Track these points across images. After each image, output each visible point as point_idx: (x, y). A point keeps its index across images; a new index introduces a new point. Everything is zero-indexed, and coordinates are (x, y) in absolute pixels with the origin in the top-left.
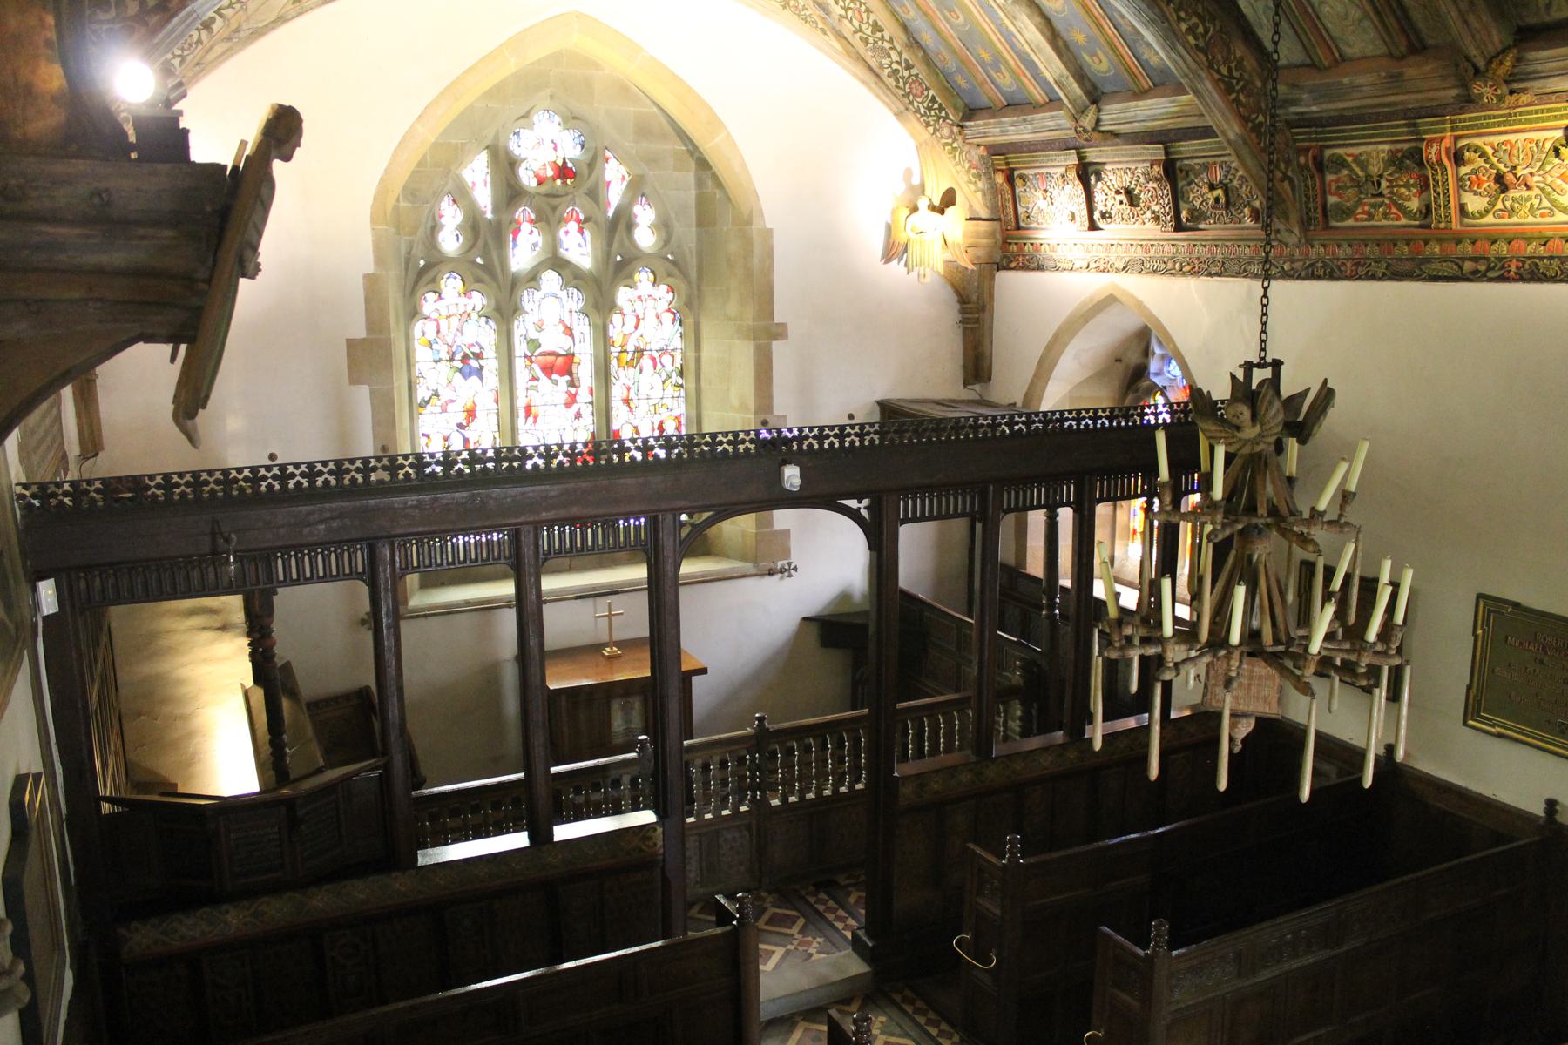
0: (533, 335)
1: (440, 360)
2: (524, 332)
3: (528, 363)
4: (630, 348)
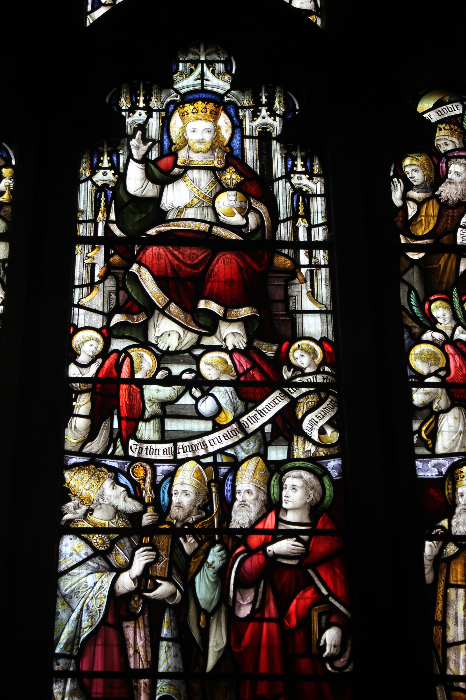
3: (116, 259)
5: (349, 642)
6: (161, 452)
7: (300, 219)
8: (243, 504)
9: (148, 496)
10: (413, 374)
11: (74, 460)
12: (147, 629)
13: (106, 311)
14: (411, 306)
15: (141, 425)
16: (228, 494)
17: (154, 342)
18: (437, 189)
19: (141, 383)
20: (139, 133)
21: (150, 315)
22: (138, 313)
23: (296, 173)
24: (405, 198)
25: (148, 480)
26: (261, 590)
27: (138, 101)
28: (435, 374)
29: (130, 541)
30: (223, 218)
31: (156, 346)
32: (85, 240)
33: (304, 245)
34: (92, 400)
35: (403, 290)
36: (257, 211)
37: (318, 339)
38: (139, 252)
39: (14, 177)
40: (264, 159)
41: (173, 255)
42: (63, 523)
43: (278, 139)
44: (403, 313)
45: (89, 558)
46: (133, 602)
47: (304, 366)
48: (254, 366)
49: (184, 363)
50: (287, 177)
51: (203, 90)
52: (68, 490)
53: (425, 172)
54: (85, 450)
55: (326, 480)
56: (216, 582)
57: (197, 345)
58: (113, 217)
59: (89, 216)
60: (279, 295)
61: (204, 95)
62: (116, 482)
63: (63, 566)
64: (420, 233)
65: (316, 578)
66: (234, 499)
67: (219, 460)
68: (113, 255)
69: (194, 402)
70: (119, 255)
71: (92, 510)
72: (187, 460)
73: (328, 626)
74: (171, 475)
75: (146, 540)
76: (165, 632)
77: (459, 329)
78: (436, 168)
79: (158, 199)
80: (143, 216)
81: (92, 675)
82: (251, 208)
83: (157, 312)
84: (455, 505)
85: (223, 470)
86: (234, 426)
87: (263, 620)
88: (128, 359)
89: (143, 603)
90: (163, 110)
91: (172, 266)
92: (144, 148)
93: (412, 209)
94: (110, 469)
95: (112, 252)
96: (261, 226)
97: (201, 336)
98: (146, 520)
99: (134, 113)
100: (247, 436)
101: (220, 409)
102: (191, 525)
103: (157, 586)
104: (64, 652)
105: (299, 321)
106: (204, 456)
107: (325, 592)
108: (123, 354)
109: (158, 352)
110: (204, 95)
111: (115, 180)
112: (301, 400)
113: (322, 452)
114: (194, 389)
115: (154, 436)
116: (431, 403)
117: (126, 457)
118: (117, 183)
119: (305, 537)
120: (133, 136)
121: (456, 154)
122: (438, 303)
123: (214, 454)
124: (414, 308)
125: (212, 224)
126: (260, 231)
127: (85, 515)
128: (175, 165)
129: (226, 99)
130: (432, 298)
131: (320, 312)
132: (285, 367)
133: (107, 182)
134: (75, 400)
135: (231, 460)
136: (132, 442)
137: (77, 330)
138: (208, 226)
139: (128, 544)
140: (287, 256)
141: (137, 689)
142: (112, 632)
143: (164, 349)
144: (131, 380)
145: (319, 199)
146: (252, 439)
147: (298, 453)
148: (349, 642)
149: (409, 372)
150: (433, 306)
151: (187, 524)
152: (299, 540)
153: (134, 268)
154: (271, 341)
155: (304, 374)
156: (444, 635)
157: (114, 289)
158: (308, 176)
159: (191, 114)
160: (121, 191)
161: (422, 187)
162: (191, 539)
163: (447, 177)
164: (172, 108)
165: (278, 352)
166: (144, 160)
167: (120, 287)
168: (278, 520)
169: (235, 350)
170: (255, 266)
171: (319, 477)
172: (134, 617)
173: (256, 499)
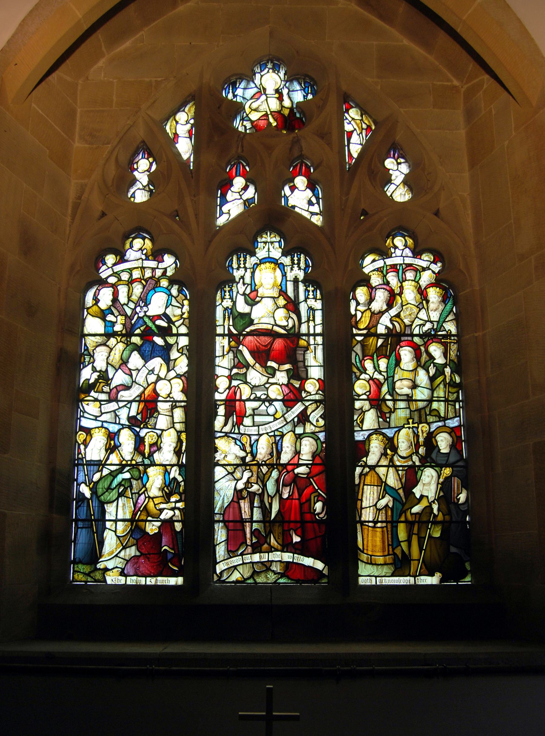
0: (242, 307)
1: (114, 334)
2: (227, 303)
3: (233, 343)
4: (381, 329)
5: (325, 508)
6: (253, 431)
7: (311, 321)
8: (286, 453)
9: (248, 449)
10: (356, 394)
11: (218, 435)
12: (249, 503)
13: (229, 368)
14: (356, 362)
15: (245, 418)
16: (279, 448)
17: (250, 382)
18: (370, 305)
19: (244, 401)
20: (242, 280)
21: (247, 369)
22: (242, 368)
23: (309, 298)
24: (356, 310)
25: (248, 443)
26: (292, 487)
27: (240, 264)
28: (365, 394)
29: (242, 468)
30: (278, 323)
31: (250, 383)
32: (220, 335)
33: (312, 335)
34: (225, 408)
35: (354, 355)
36: (292, 318)
37: (317, 379)
38: (242, 340)
39: (190, 305)
40: (296, 291)
41: (257, 340)
42: (215, 461)
43: (302, 281)
44: (353, 366)
45: (226, 475)
46: (243, 493)
47: (310, 391)
48: (291, 391)
49: (262, 391)
50: (306, 301)
51: (269, 257)
52: (217, 448)
53: (366, 297)
54: (223, 431)
55: (318, 441)
56: (275, 484)
57: (267, 383)
58: (231, 323)
59: (222, 324)
60: (300, 358)
61: (269, 260)
62: (236, 443)
63: (216, 479)
64: (362, 327)
65: (313, 483)
66: (282, 450)
67: (276, 434)
68: (232, 341)
69: (266, 408)
70: (234, 341)
71: (227, 456)
72: (263, 434)
73: (318, 501)
74: (257, 440)
75: (248, 468)
76: (256, 504)
77: (376, 373)
78: (371, 294)
79: (249, 314)
80: (244, 322)
81: (229, 521)
82: (290, 317)
83: (250, 368)
84: (369, 452)
85: (278, 438)
86: (282, 419)
87: (293, 499)
88: (239, 389)
89: (247, 493)
90: (252, 268)
91: (256, 346)
92: (244, 288)
93: (359, 315)
94: (233, 438)
95: (231, 340)
96: (294, 326)
97: (269, 378)
98: (248, 459)
99: (239, 270)
100: (287, 423)
101: (277, 411)
102: (265, 462)
103: (252, 486)
104: (218, 512)
105: (309, 371)
106: (270, 432)
107: (317, 488)
108: (237, 388)
109: (251, 386)
110: (269, 260)
111: (232, 305)
112: (309, 407)
113: (317, 430)
114: (266, 402)
115: (251, 424)
116: (362, 407)
117: (239, 433)
118: (232, 306)
119: (310, 466)
120: (239, 282)
121: (380, 287)
122: (368, 360)
123: (274, 431)
124: (358, 363)
125: (273, 325)
126: (294, 328)
127: (224, 458)
128: (257, 296)
129: (279, 262)
130: (365, 359)
131: (319, 366)
132: (303, 392)
133: (228, 306)
134: (218, 408)
135: (281, 434)
136: (241, 427)
137: (218, 377)
138: (272, 326)
139: (241, 469)
140: (305, 340)
141: (246, 526)
142: (236, 505)
143: (254, 385)
144: (240, 400)
145: (319, 311)
146: (289, 424)
147: (308, 430)
148: (325, 508)
149: (354, 394)
150: (366, 362)
151: (264, 461)
152: (307, 467)
153: (241, 346)
154: (298, 380)
155: (311, 395)
156: (361, 505)
157: (232, 358)
158: (314, 300)
159: (264, 269)
160: (234, 310)
161: (364, 304)
162: (265, 467)
163: (375, 299)
164: (255, 266)
165: (300, 385)
166: (244, 294)
167: (235, 356)
168: (299, 458)
169: (283, 384)
170: (292, 346)
171: (316, 440)
172: (244, 498)
173: (291, 450)
